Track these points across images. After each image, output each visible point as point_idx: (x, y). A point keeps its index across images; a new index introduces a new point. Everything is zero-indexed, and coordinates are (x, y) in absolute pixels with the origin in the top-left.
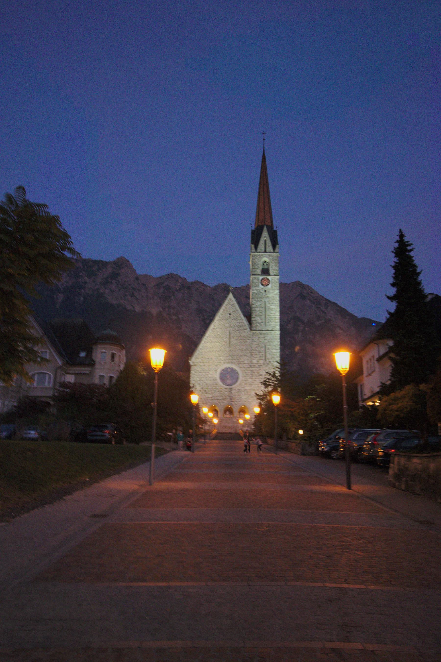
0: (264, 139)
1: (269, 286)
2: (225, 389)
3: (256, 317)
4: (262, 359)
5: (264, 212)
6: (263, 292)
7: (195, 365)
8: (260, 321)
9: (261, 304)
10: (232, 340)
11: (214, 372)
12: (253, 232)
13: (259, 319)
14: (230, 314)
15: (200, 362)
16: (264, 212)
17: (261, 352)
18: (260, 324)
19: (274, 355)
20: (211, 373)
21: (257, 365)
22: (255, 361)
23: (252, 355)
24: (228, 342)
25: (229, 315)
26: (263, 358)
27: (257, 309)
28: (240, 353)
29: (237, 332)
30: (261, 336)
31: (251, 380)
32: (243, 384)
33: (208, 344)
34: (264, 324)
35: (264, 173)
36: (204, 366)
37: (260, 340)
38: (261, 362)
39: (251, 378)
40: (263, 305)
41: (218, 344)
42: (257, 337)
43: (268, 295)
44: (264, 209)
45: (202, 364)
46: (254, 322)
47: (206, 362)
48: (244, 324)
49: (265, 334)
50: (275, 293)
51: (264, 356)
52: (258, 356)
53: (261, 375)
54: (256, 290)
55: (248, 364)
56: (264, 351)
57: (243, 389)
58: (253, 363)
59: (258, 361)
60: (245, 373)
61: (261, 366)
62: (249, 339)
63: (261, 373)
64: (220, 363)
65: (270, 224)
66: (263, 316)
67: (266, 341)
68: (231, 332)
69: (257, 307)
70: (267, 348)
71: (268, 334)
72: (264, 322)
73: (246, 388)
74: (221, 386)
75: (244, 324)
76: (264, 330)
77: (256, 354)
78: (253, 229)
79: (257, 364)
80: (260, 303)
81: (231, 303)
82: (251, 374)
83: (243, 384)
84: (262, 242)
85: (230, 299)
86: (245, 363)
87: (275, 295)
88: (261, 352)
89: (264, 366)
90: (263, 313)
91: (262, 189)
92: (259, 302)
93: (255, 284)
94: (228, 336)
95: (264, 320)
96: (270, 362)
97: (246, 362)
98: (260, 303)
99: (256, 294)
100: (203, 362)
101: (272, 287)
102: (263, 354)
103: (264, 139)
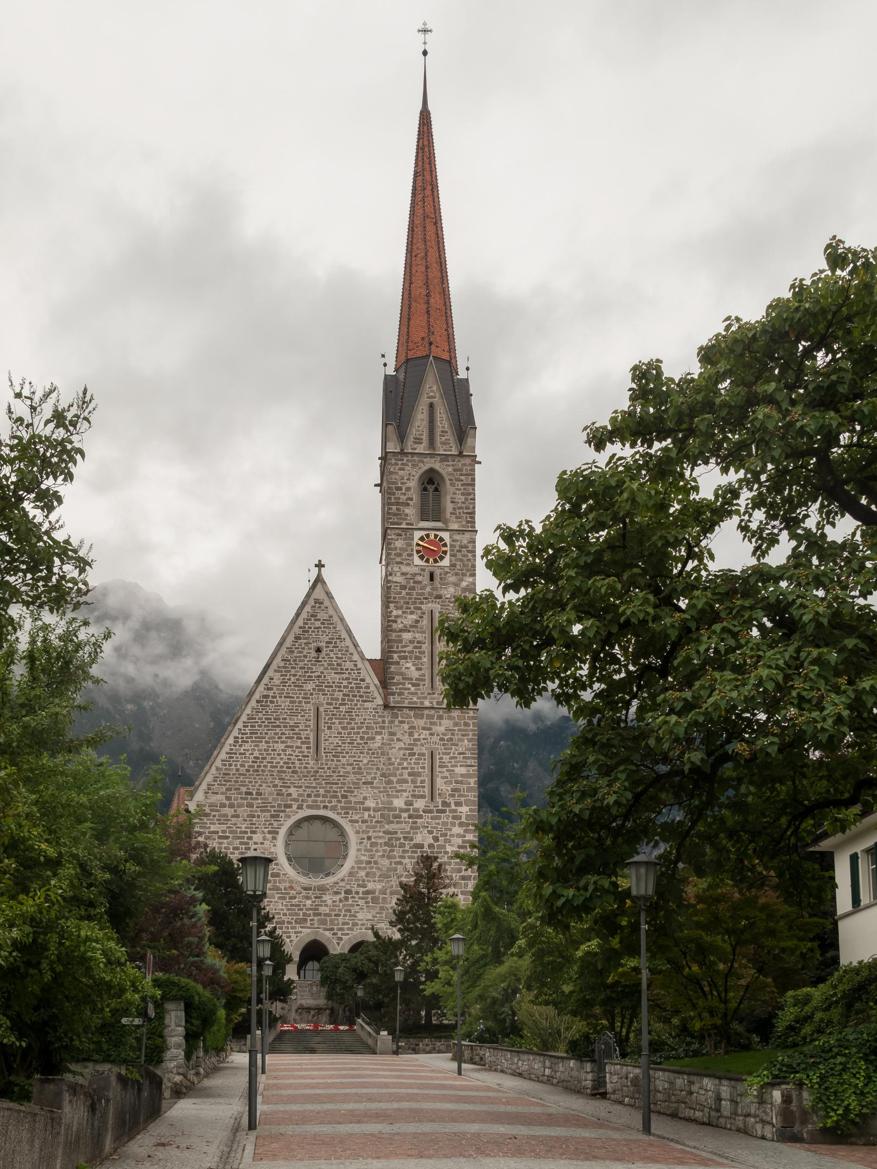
0: (425, 53)
1: (446, 562)
2: (305, 889)
3: (402, 662)
4: (423, 797)
5: (428, 312)
6: (426, 580)
7: (207, 815)
8: (415, 674)
9: (417, 621)
10: (325, 733)
11: (269, 836)
12: (388, 381)
13: (413, 668)
14: (319, 650)
15: (223, 805)
16: (428, 312)
17: (419, 774)
18: (413, 685)
19: (457, 782)
20: (257, 837)
21: (405, 815)
22: (399, 803)
23: (390, 782)
24: (312, 739)
25: (314, 654)
26: (427, 791)
27: (407, 636)
28: (352, 777)
29: (343, 709)
30: (421, 723)
31: (386, 862)
32: (362, 873)
33: (246, 746)
34: (427, 682)
35: (428, 177)
36: (237, 816)
37: (416, 736)
38: (420, 804)
39: (389, 857)
40: (425, 622)
41: (282, 746)
42: (406, 726)
43: (443, 592)
44: (428, 302)
45: (229, 811)
46: (397, 679)
47: (240, 806)
48: (363, 684)
49: (432, 717)
50: (464, 584)
51: (427, 784)
52: (409, 786)
53: (422, 846)
54: (403, 574)
55: (375, 810)
56: (427, 771)
57: (361, 890)
58: (395, 809)
59: (409, 803)
60: (369, 838)
61: (421, 817)
62: (377, 733)
63: (418, 839)
64: (290, 806)
65: (446, 356)
66: (426, 659)
67: (435, 738)
68: (321, 709)
69: (405, 630)
70: (437, 763)
71: (440, 717)
72: (427, 677)
73: (370, 886)
74: (291, 881)
75: (363, 684)
76: (427, 703)
77: (406, 781)
78: (391, 371)
79: (407, 810)
80: (414, 617)
81: (322, 615)
82: (386, 844)
83: (362, 873)
84: (420, 418)
85: (317, 601)
86: (368, 809)
87: (465, 590)
88: (419, 774)
89: (427, 819)
90: (426, 647)
91: (419, 235)
92: (412, 613)
93: (400, 555)
94: (312, 723)
95: (427, 673)
96: (445, 804)
97: (370, 803)
98: (414, 617)
99: (403, 587)
100: (231, 806)
101: (453, 565)
102: (427, 780)
103: (425, 53)
